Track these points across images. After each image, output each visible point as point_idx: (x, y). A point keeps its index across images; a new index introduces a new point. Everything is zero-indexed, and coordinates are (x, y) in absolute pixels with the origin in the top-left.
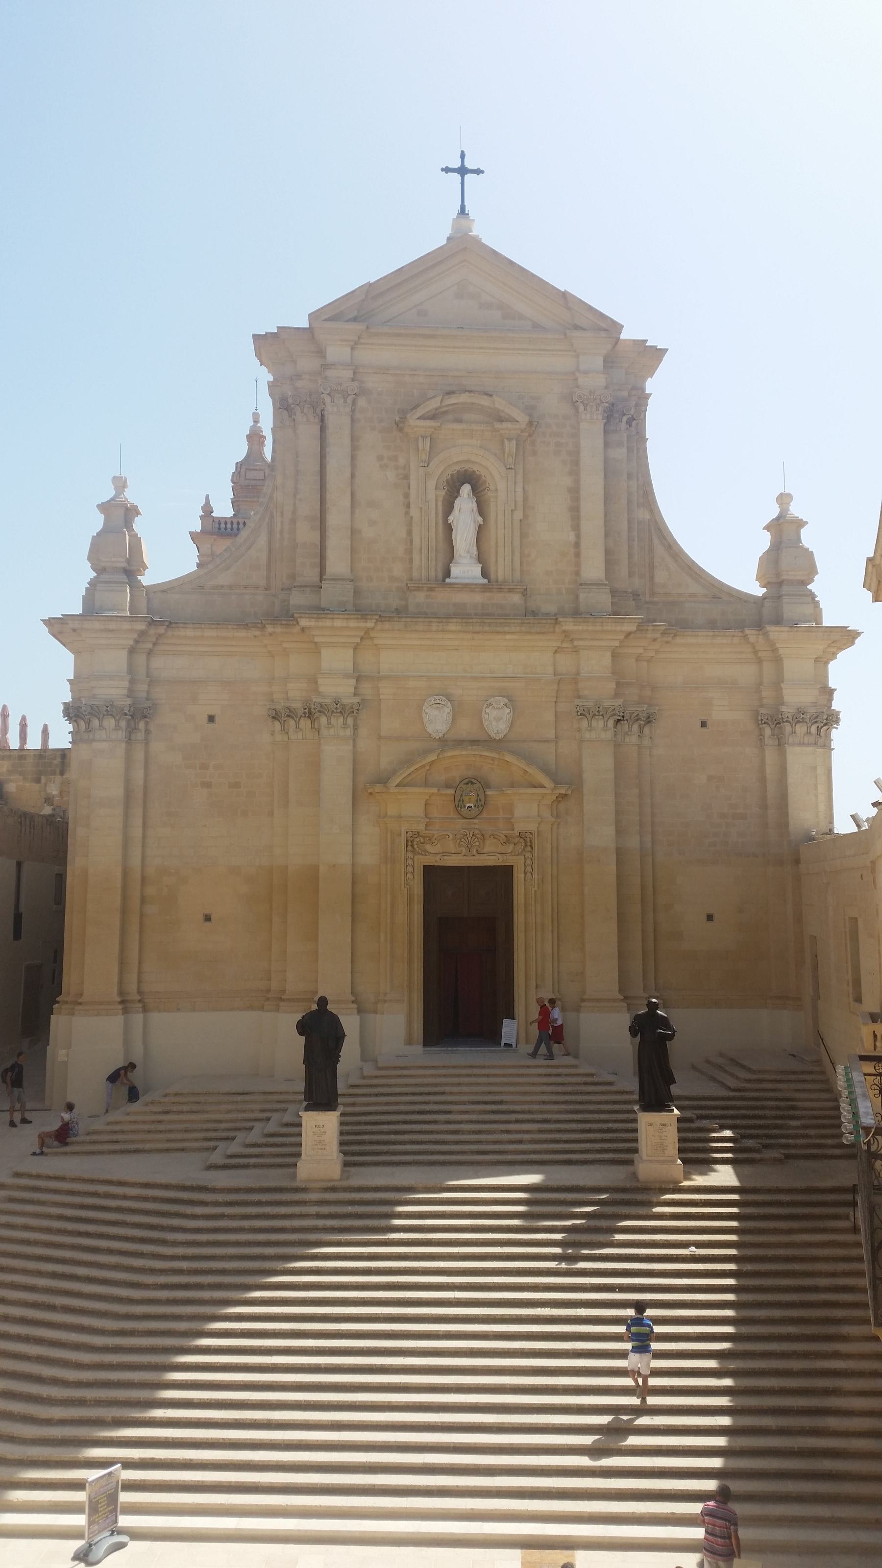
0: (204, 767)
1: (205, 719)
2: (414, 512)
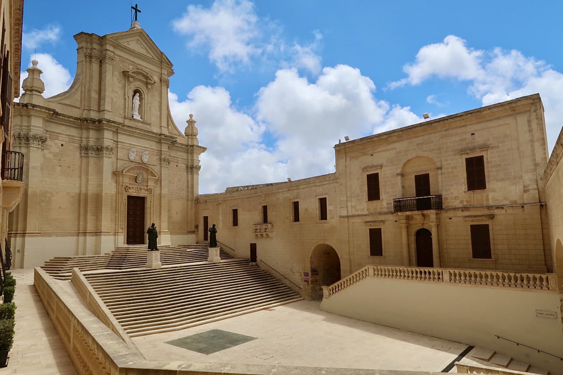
0: (60, 160)
1: (61, 145)
2: (127, 97)
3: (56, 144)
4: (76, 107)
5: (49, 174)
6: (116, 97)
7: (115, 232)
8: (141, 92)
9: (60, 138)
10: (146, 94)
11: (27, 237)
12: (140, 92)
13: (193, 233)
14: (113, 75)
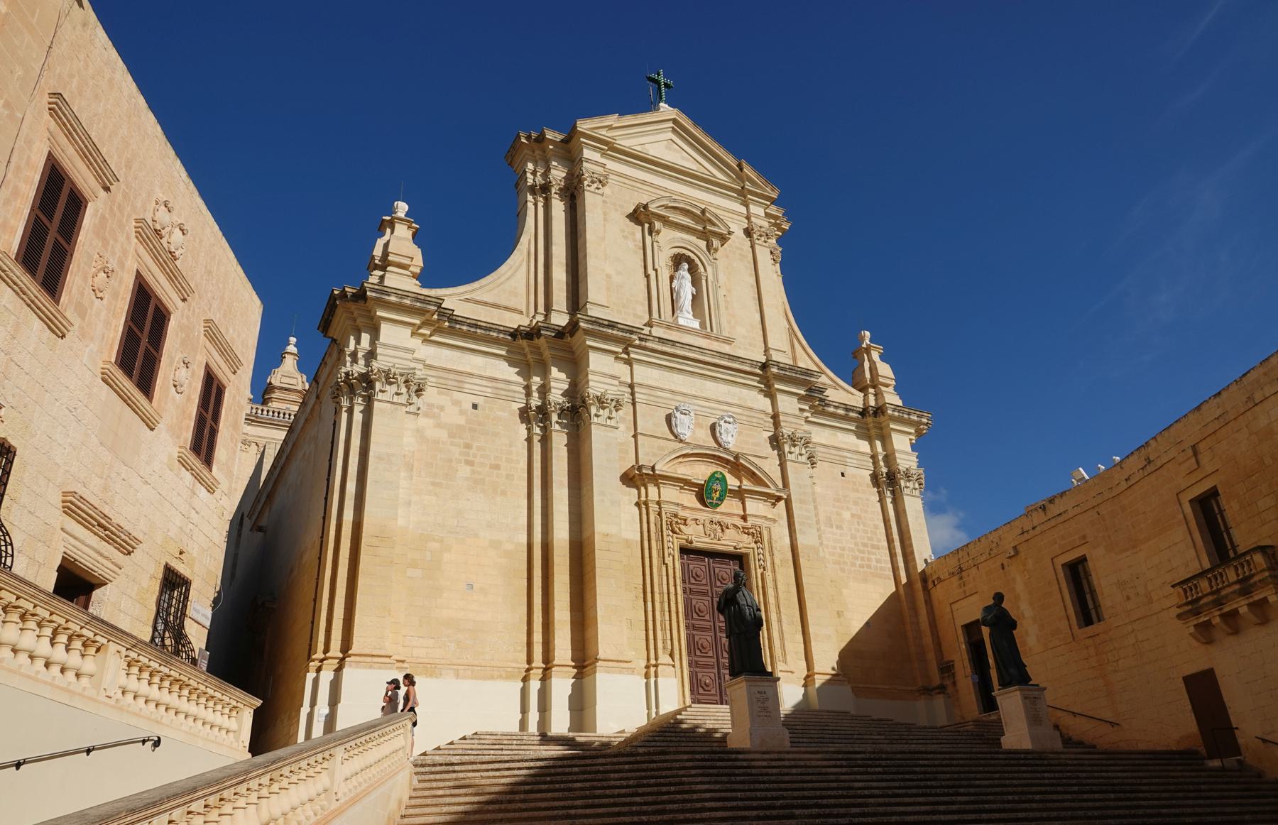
0: (468, 446)
3: (456, 403)
4: (513, 310)
5: (434, 484)
7: (647, 667)
8: (693, 260)
9: (467, 386)
10: (708, 264)
11: (350, 666)
12: (690, 262)
13: (939, 693)
14: (605, 220)
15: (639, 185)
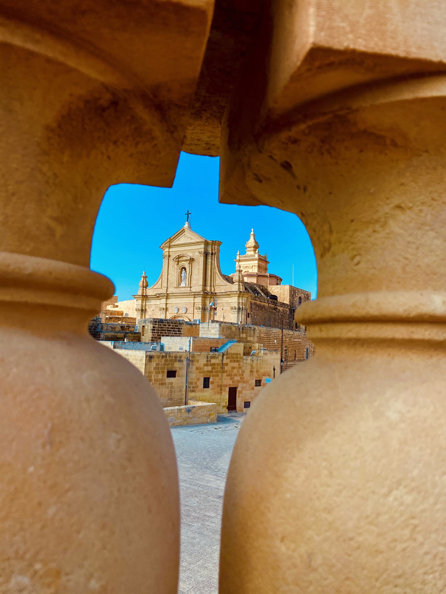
3: (150, 310)
6: (171, 277)
9: (152, 307)
15: (176, 252)
